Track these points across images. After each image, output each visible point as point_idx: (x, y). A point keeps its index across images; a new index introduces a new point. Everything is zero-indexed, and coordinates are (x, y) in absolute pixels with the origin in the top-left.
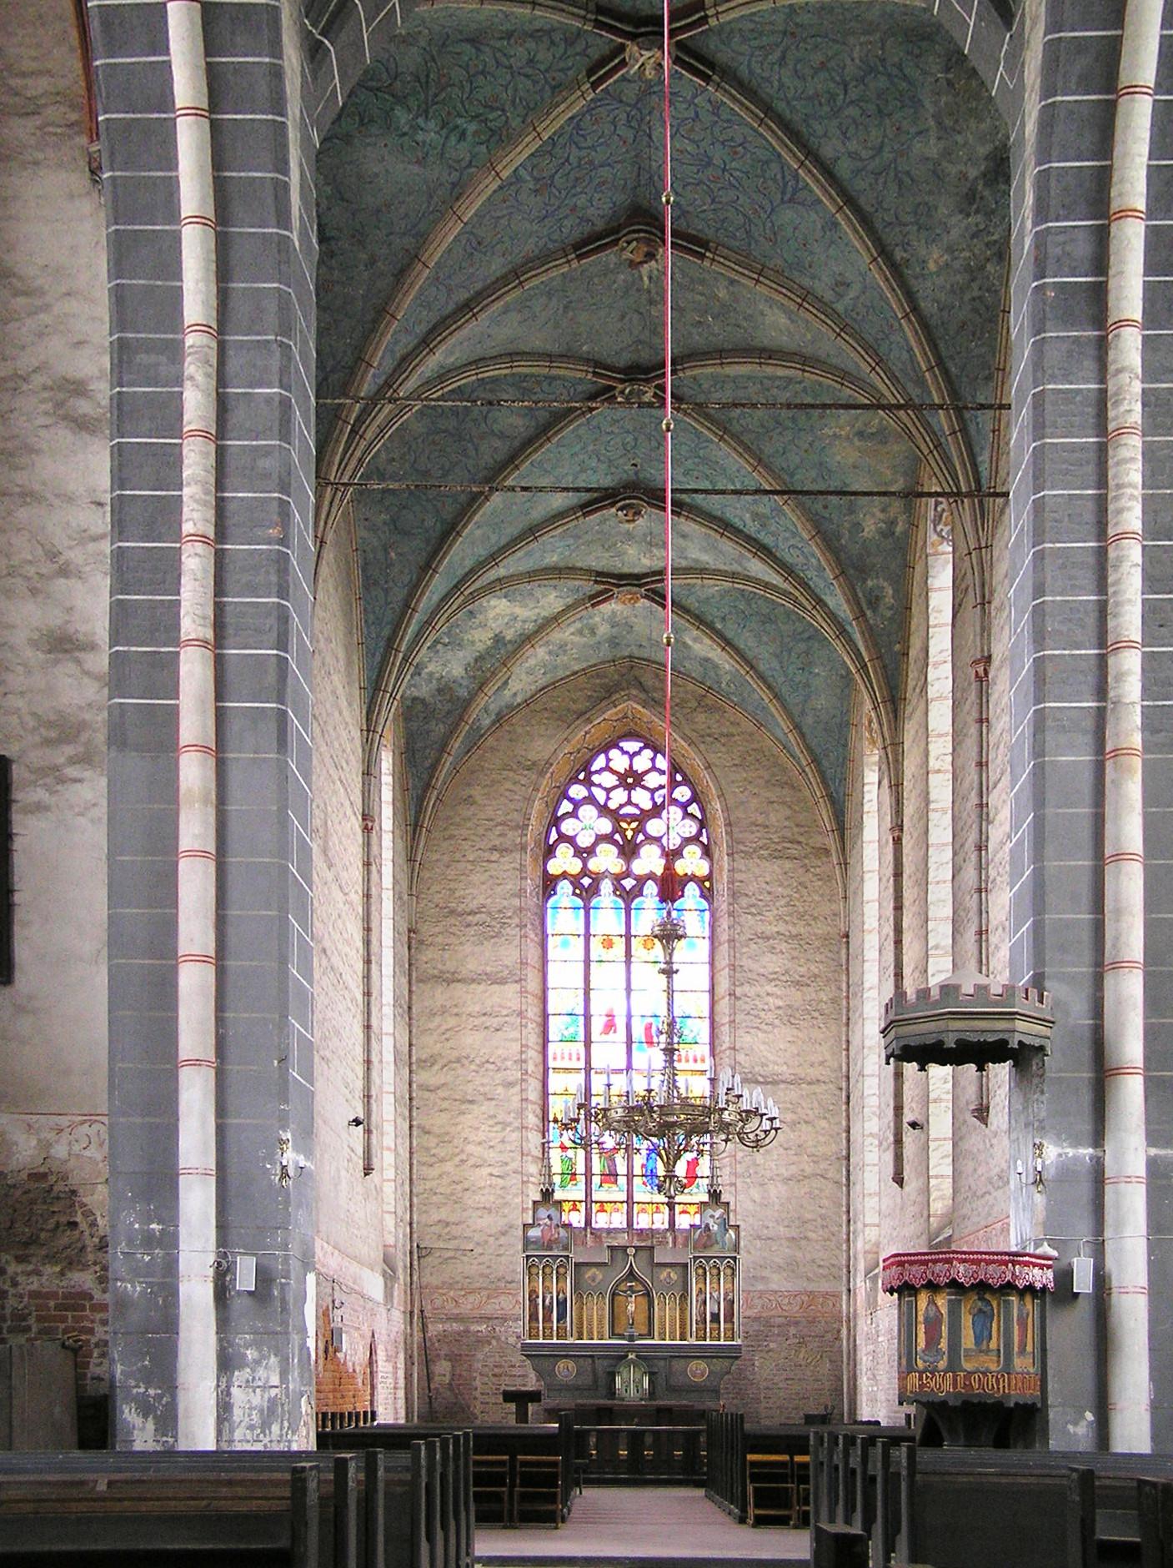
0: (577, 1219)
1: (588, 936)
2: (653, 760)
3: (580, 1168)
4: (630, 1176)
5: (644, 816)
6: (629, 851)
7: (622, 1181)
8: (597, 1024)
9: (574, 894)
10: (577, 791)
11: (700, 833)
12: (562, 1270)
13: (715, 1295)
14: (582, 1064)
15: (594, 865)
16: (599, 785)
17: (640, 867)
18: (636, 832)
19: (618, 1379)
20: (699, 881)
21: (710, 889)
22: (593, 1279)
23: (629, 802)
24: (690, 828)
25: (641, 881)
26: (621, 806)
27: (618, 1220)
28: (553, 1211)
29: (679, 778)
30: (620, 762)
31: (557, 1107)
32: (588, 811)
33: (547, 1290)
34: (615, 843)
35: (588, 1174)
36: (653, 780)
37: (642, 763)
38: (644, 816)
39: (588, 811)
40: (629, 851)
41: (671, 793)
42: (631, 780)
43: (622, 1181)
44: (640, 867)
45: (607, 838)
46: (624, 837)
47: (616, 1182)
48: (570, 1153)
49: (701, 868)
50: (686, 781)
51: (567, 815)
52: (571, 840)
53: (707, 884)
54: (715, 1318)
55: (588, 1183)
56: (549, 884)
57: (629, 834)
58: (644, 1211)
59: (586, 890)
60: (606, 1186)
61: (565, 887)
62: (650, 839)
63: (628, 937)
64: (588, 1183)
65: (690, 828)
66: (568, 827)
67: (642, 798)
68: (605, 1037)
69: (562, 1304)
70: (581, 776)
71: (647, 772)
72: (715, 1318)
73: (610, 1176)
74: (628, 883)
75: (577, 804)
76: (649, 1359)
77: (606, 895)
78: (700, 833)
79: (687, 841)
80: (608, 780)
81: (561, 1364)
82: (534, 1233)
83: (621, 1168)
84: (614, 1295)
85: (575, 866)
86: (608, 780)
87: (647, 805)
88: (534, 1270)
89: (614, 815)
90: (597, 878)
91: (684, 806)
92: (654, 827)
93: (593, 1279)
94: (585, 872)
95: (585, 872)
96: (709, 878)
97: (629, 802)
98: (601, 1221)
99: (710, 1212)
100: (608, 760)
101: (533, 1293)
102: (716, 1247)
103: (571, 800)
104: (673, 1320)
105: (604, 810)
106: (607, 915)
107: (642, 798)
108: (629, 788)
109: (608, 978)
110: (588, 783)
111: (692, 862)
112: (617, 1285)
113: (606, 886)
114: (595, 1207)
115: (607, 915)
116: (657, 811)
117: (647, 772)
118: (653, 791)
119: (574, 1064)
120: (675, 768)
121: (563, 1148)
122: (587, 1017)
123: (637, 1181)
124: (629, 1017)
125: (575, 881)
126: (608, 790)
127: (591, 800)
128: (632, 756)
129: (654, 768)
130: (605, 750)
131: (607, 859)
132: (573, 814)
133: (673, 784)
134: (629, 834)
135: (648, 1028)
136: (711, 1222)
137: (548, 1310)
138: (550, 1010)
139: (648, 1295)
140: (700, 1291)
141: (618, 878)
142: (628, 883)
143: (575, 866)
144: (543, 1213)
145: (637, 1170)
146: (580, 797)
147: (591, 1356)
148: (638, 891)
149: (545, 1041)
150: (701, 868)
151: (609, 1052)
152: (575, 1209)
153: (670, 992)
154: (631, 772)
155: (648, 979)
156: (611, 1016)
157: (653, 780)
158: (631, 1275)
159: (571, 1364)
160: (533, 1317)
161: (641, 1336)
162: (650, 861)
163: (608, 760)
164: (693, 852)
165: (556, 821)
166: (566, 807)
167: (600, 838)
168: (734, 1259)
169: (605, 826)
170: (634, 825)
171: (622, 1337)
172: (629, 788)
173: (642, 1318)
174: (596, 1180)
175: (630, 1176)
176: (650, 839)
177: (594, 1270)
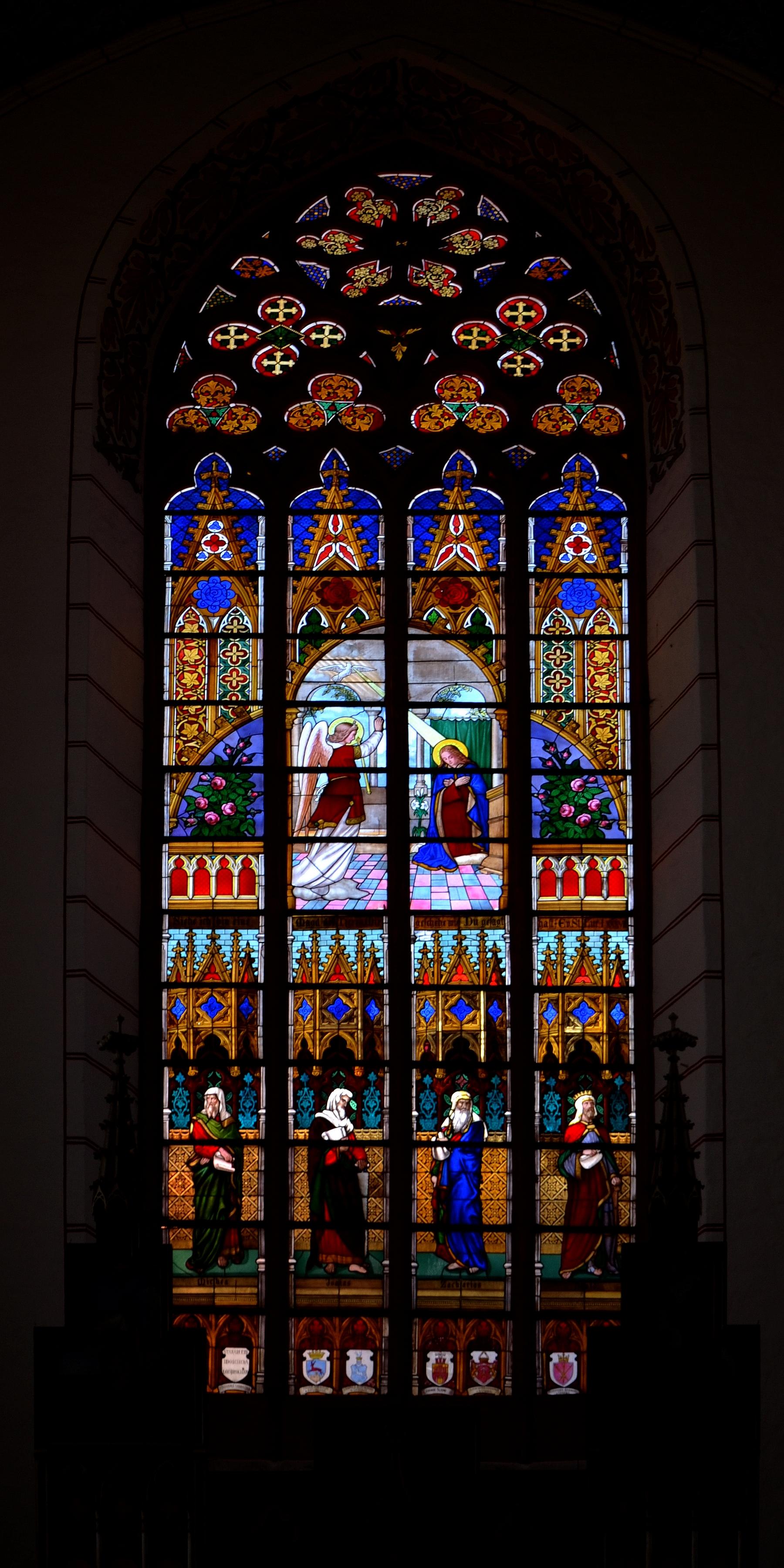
3: (253, 1207)
7: (376, 1240)
14: (258, 898)
16: (318, 254)
45: (337, 359)
55: (277, 1252)
57: (399, 352)
63: (395, 577)
64: (277, 1252)
83: (376, 1208)
89: (361, 315)
119: (235, 899)
122: (279, 769)
123: (423, 1243)
131: (334, 403)
134: (399, 352)
135: (453, 801)
145: (423, 1207)
153: (515, 704)
156: (343, 766)
175: (401, 1225)
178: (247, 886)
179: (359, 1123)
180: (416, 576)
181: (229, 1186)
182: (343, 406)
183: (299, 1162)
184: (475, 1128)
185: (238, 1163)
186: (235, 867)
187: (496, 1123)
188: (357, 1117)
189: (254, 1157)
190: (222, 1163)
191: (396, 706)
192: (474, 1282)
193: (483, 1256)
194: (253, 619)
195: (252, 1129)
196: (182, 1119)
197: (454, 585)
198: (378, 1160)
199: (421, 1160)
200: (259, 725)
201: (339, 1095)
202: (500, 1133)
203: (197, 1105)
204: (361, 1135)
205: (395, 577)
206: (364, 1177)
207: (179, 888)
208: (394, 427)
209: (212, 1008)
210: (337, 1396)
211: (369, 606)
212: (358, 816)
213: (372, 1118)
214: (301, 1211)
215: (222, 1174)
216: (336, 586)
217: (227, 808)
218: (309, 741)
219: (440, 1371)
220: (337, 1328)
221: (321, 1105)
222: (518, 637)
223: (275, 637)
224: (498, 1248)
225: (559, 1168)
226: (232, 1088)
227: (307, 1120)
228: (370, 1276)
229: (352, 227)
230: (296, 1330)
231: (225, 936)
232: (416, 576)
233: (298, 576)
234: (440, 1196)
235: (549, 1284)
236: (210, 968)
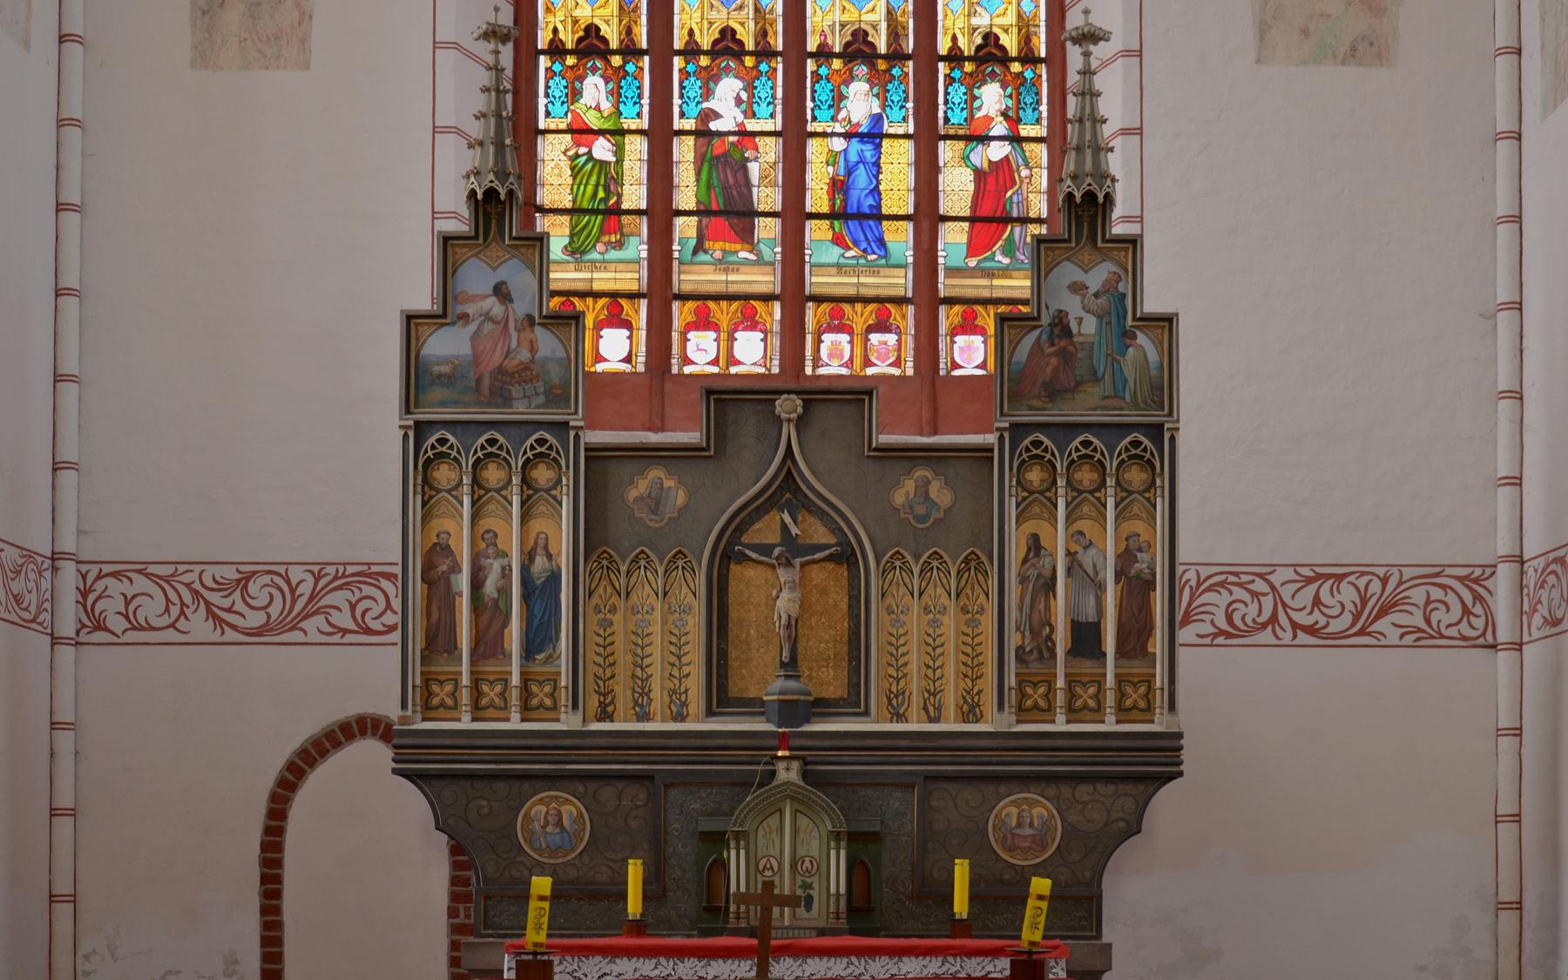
3: (635, 195)
4: (794, 215)
7: (768, 230)
12: (542, 474)
19: (736, 861)
22: (655, 501)
33: (486, 544)
35: (661, 212)
43: (768, 230)
47: (746, 236)
48: (602, 149)
54: (1086, 638)
60: (716, 248)
69: (539, 593)
72: (1086, 638)
73: (731, 213)
76: (835, 777)
81: (537, 809)
83: (767, 197)
84: (727, 556)
93: (655, 501)
104: (933, 646)
121: (580, 132)
123: (817, 232)
137: (489, 614)
139: (846, 556)
145: (817, 198)
147: (648, 777)
159: (571, 809)
160: (438, 640)
161: (822, 707)
171: (752, 706)
173: (824, 639)
174: (685, 228)
175: (794, 215)
177: (656, 473)
179: (750, 114)
181: (610, 176)
183: (684, 151)
184: (877, 119)
187: (896, 114)
189: (637, 148)
190: (602, 149)
192: (873, 269)
193: (881, 243)
195: (636, 117)
196: (558, 109)
198: (770, 150)
199: (816, 151)
201: (729, 88)
202: (900, 122)
203: (574, 94)
204: (751, 125)
206: (754, 168)
213: (763, 110)
214: (686, 195)
215: (603, 164)
219: (835, 352)
220: (723, 313)
221: (707, 94)
224: (900, 239)
225: (965, 159)
226: (615, 78)
227: (693, 110)
228: (760, 262)
230: (681, 313)
234: (838, 186)
235: (952, 272)
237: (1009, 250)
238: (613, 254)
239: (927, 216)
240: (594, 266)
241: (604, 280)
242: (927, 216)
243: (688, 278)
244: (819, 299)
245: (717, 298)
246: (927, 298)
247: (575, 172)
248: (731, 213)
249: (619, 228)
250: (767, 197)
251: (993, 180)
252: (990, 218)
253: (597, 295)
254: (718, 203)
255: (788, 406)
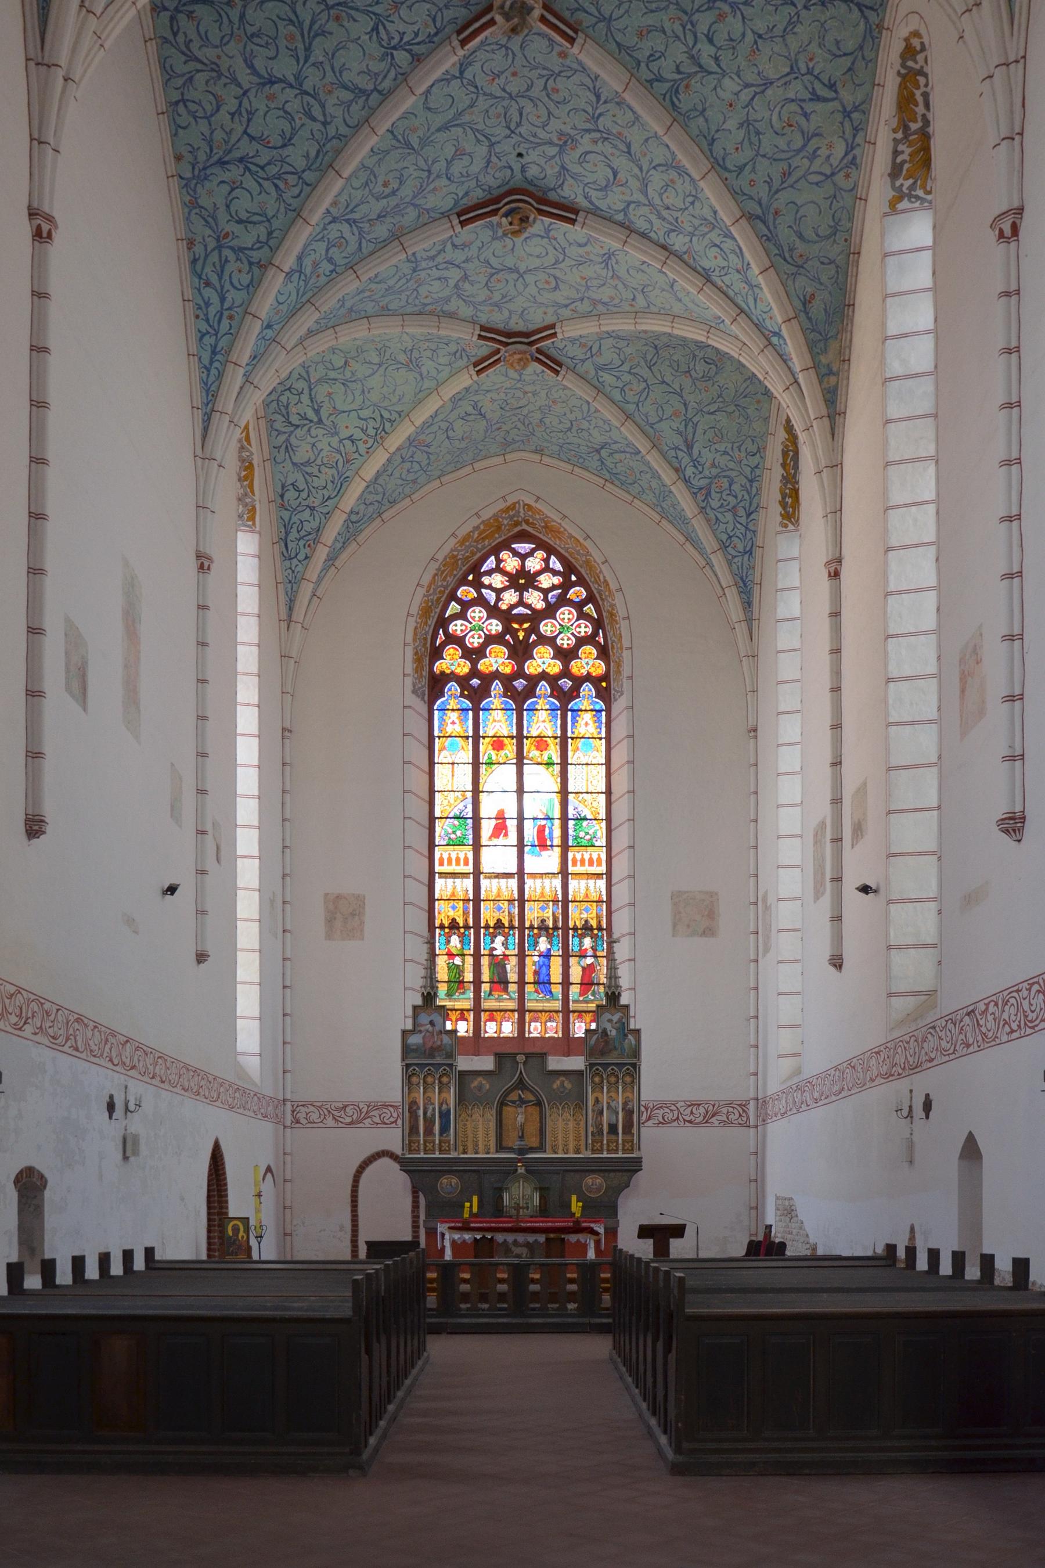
0: (463, 1028)
1: (476, 738)
2: (546, 561)
3: (469, 976)
4: (522, 983)
5: (537, 617)
6: (521, 652)
7: (513, 988)
8: (487, 827)
9: (462, 695)
10: (466, 592)
11: (595, 634)
13: (613, 1104)
15: (483, 665)
16: (490, 587)
17: (532, 667)
18: (528, 632)
20: (595, 681)
21: (608, 689)
23: (521, 603)
24: (585, 629)
25: (533, 681)
26: (512, 607)
27: (508, 1029)
28: (437, 1018)
29: (574, 578)
30: (511, 564)
31: (444, 912)
32: (477, 613)
34: (506, 644)
35: (477, 982)
36: (546, 581)
37: (534, 564)
38: (537, 617)
39: (477, 613)
40: (521, 652)
41: (566, 592)
42: (522, 580)
43: (513, 988)
44: (532, 667)
46: (515, 636)
47: (506, 990)
48: (458, 961)
49: (598, 668)
50: (581, 582)
51: (455, 617)
52: (459, 641)
53: (604, 684)
56: (436, 685)
58: (536, 1020)
59: (476, 692)
60: (496, 994)
61: (453, 687)
62: (543, 640)
63: (520, 738)
65: (585, 629)
66: (457, 627)
67: (535, 599)
68: (495, 841)
70: (470, 578)
71: (539, 573)
74: (520, 684)
75: (466, 605)
77: (496, 698)
78: (595, 634)
79: (581, 641)
80: (498, 581)
82: (415, 1040)
83: (513, 976)
85: (463, 668)
86: (498, 581)
87: (540, 605)
88: (414, 1079)
89: (506, 617)
90: (488, 679)
91: (579, 606)
92: (547, 628)
94: (474, 673)
95: (474, 673)
96: (606, 677)
97: (521, 603)
98: (490, 1029)
99: (607, 1016)
100: (499, 561)
101: (413, 1106)
102: (615, 1053)
103: (459, 601)
105: (493, 611)
106: (498, 721)
107: (535, 599)
108: (521, 589)
109: (500, 778)
110: (478, 585)
111: (588, 662)
112: (508, 1092)
113: (497, 687)
114: (484, 1016)
115: (498, 721)
116: (550, 611)
117: (539, 573)
118: (545, 592)
120: (569, 568)
121: (450, 955)
122: (477, 819)
123: (529, 988)
124: (521, 819)
125: (463, 681)
126: (499, 592)
127: (481, 601)
128: (523, 557)
129: (546, 569)
130: (496, 551)
132: (462, 615)
133: (566, 586)
136: (608, 1026)
138: (437, 814)
140: (597, 1101)
141: (507, 681)
142: (520, 684)
143: (463, 668)
144: (424, 1019)
146: (470, 597)
148: (530, 692)
149: (432, 845)
150: (598, 668)
151: (499, 857)
152: (463, 1018)
154: (522, 572)
155: (541, 779)
156: (501, 817)
157: (546, 581)
158: (521, 1084)
162: (543, 661)
163: (499, 561)
164: (588, 651)
165: (443, 623)
166: (454, 607)
167: (491, 639)
168: (634, 1066)
169: (495, 626)
170: (526, 626)
172: (521, 589)
174: (485, 987)
175: (522, 983)
176: (543, 640)
178: (466, 863)
180: (527, 738)
182: (500, 661)
185: (463, 962)
186: (462, 856)
188: (505, 944)
190: (458, 961)
191: (520, 791)
192: (548, 1001)
193: (551, 992)
194: (467, 756)
196: (443, 947)
197: (541, 742)
200: (470, 800)
205: (520, 738)
207: (441, 864)
208: (519, 673)
209: (454, 908)
210: (499, 1037)
211: (510, 749)
212: (506, 835)
214: (486, 976)
216: (498, 744)
217: (458, 833)
218: (489, 807)
222: (564, 763)
223: (476, 764)
224: (557, 990)
228: (511, 998)
229: (504, 573)
231: (458, 881)
232: (527, 738)
233: (484, 738)
235: (574, 1002)
236: (453, 894)
237: (593, 994)
238: (462, 996)
239: (566, 983)
240: (455, 1000)
241: (458, 1005)
242: (566, 983)
243: (486, 1005)
244: (530, 1011)
245: (496, 1011)
246: (566, 1011)
247: (449, 968)
248: (500, 982)
249: (463, 988)
250: (513, 976)
251: (588, 970)
252: (587, 983)
253: (456, 1010)
254: (496, 979)
255: (521, 1058)
